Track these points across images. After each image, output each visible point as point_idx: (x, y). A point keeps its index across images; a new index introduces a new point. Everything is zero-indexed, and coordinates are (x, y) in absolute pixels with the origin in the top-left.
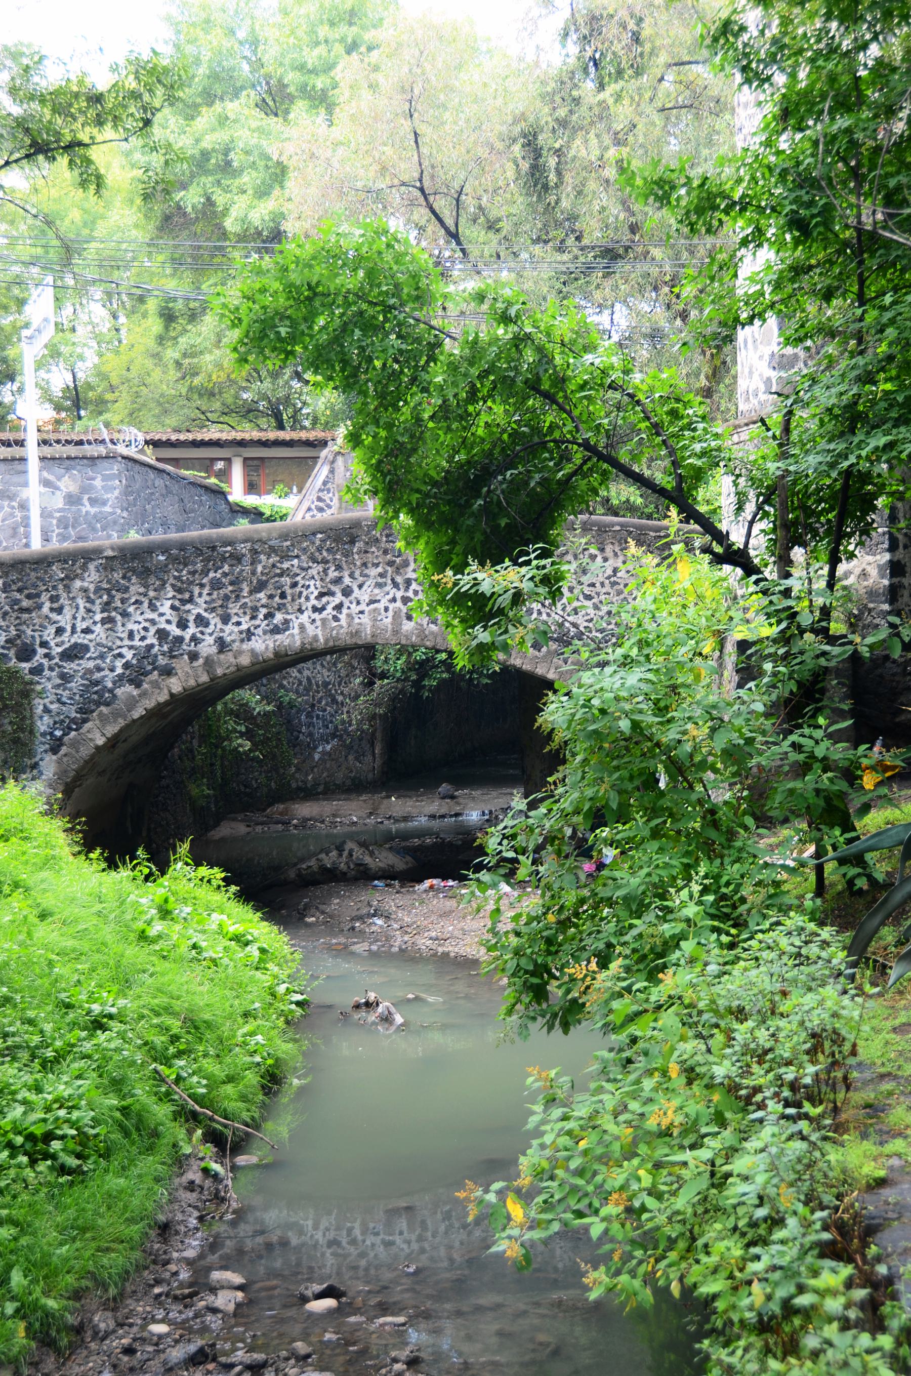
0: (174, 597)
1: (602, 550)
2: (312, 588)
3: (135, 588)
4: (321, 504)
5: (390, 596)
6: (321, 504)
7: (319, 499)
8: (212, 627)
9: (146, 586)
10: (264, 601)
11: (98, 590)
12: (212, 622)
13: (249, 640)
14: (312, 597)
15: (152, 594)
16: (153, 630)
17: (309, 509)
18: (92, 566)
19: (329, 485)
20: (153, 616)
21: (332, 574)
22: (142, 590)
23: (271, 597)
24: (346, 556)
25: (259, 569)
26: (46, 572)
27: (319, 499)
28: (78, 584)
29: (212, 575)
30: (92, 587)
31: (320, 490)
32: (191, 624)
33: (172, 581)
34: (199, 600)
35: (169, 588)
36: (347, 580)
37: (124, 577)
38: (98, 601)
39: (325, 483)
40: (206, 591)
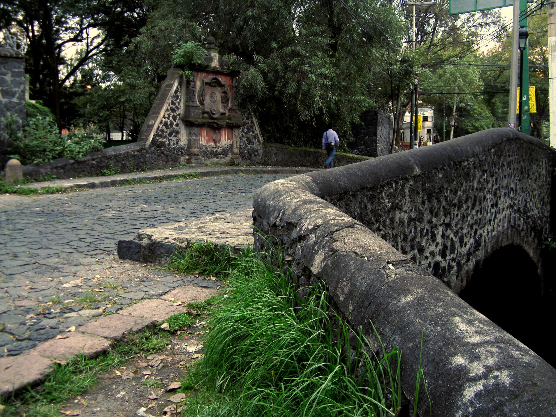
0: (444, 220)
1: (542, 162)
2: (489, 200)
3: (427, 216)
4: (173, 106)
5: (506, 205)
6: (173, 106)
7: (173, 103)
8: (456, 252)
9: (431, 211)
10: (475, 218)
11: (411, 219)
12: (456, 247)
13: (468, 260)
14: (489, 211)
15: (434, 220)
16: (432, 265)
17: (167, 110)
18: (407, 190)
19: (179, 94)
20: (432, 248)
21: (494, 187)
22: (429, 217)
23: (477, 212)
24: (499, 169)
25: (475, 185)
26: (380, 204)
27: (173, 103)
28: (398, 215)
29: (459, 193)
30: (405, 217)
31: (174, 97)
32: (448, 252)
33: (444, 203)
34: (453, 223)
35: (442, 213)
36: (498, 192)
37: (423, 203)
38: (410, 237)
39: (176, 92)
40: (456, 213)
